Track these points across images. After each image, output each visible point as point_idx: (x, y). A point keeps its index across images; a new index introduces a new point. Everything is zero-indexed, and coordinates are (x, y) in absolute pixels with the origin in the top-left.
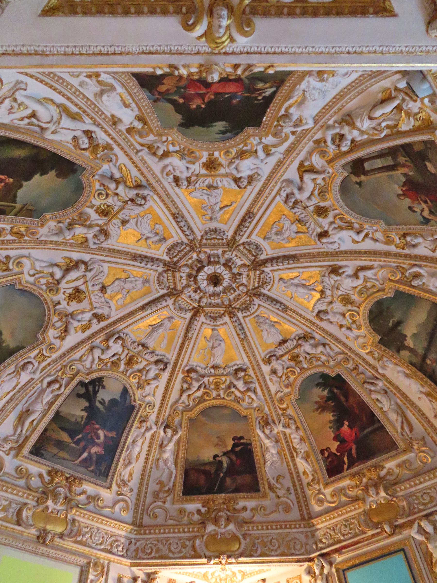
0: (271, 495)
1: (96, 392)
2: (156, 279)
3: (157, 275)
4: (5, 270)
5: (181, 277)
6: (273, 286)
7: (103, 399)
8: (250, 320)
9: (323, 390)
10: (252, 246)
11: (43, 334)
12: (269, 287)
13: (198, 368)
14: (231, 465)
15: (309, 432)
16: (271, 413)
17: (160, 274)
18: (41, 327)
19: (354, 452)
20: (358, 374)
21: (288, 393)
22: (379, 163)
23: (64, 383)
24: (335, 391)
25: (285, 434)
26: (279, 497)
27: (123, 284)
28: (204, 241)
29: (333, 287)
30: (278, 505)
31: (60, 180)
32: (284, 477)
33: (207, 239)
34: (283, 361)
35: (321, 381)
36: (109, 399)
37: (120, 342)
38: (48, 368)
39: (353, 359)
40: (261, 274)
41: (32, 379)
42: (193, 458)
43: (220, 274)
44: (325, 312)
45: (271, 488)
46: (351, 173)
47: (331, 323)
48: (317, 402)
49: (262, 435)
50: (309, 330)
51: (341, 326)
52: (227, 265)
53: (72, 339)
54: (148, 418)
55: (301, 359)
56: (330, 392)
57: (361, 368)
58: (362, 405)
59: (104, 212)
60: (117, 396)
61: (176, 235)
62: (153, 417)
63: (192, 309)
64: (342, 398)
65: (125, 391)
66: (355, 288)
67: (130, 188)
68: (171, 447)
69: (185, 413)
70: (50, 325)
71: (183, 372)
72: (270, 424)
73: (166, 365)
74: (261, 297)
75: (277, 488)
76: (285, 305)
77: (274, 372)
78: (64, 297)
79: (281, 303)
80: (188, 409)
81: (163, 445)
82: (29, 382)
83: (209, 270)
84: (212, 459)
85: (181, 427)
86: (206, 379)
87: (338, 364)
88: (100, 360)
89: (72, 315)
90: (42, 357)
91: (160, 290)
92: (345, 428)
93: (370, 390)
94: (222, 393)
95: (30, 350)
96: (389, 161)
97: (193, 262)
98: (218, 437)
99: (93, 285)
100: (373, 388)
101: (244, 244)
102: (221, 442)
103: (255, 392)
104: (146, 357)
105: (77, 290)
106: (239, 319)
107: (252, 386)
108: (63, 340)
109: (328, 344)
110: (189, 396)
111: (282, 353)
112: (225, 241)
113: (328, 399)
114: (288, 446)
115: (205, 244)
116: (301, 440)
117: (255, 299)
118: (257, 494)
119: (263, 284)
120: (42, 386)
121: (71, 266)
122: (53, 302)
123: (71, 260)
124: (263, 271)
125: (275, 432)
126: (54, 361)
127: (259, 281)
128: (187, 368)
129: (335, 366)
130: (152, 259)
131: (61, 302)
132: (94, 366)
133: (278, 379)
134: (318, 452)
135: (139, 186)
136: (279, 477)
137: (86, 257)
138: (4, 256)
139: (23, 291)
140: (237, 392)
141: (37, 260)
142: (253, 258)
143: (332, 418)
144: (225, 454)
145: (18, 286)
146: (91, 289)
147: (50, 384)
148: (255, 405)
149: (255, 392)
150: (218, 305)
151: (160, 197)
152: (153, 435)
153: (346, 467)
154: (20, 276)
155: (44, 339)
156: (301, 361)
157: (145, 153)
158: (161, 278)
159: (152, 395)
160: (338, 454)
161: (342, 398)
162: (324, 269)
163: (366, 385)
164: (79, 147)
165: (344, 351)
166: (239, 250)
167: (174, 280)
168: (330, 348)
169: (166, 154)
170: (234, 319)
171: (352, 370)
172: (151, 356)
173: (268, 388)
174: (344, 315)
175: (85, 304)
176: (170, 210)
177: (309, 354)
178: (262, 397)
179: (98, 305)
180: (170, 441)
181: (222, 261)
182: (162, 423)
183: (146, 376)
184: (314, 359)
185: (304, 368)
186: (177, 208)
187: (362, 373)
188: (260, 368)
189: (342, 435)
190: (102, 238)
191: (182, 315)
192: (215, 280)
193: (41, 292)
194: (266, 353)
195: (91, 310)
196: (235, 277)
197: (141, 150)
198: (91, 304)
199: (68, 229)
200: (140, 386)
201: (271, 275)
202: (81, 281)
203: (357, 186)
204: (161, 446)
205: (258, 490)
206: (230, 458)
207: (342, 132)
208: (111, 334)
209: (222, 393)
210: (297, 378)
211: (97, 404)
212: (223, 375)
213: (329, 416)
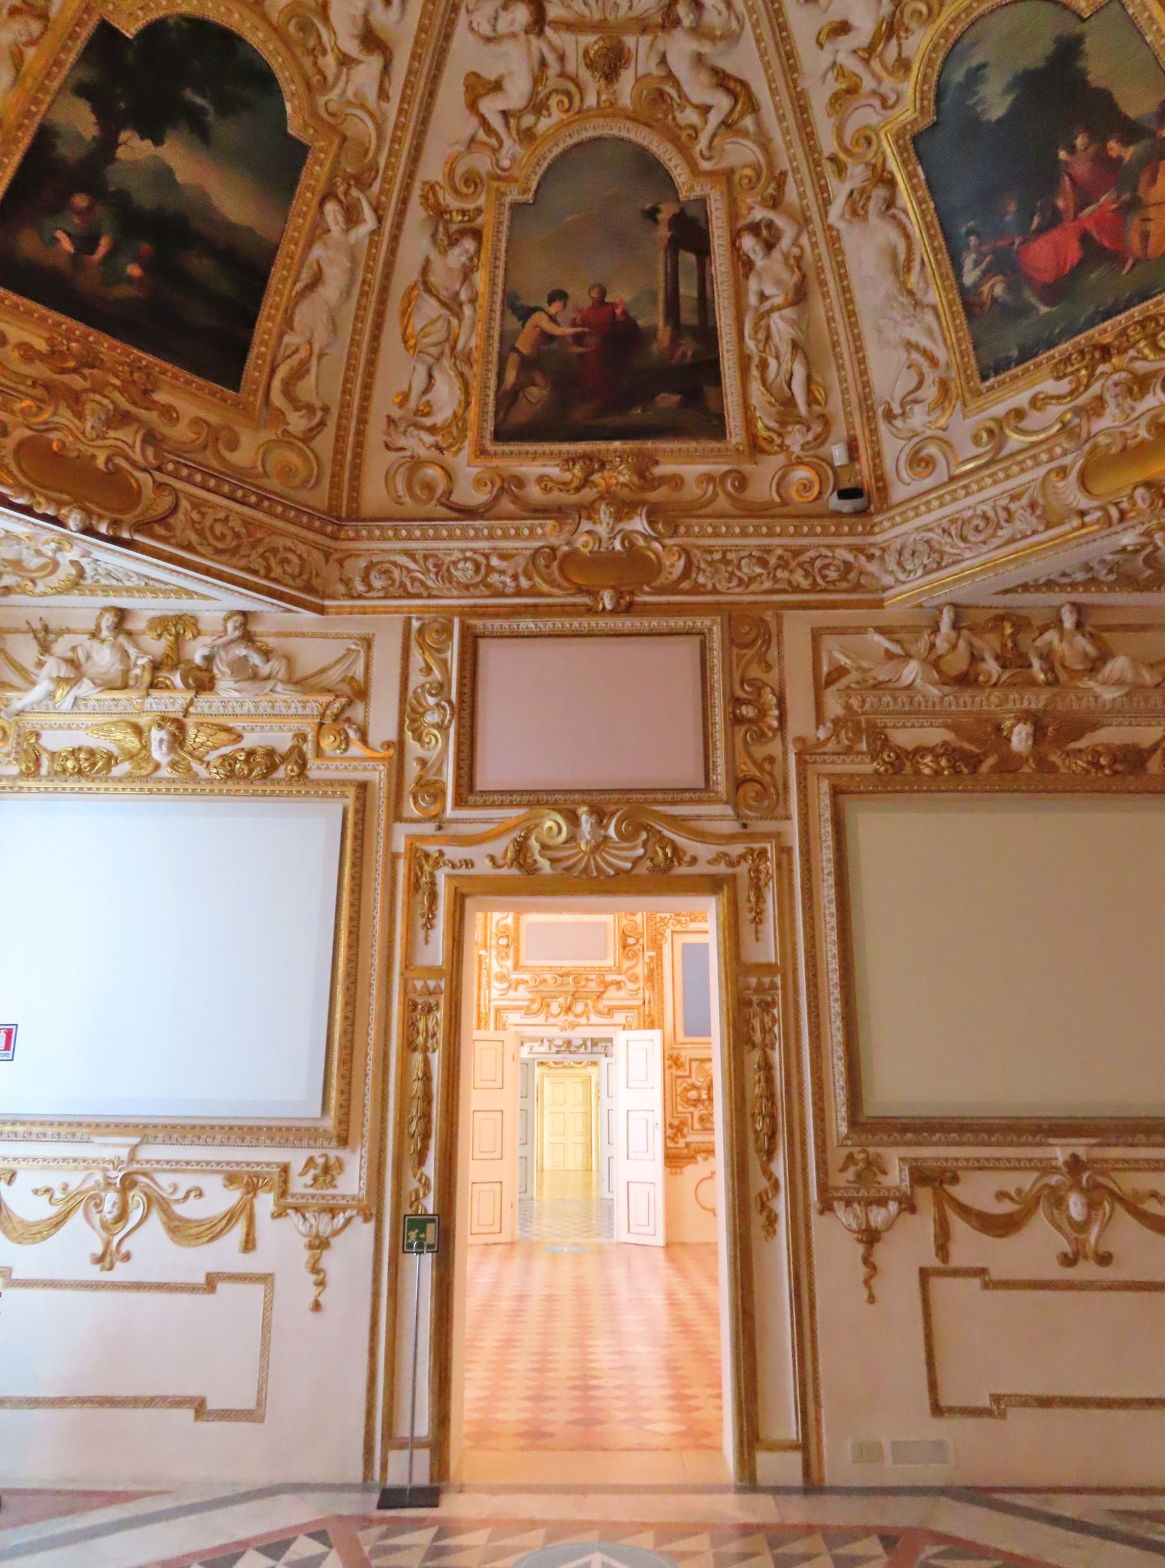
22: (688, 290)
46: (682, 211)
96: (688, 317)
203: (648, 206)
207: (776, 254)
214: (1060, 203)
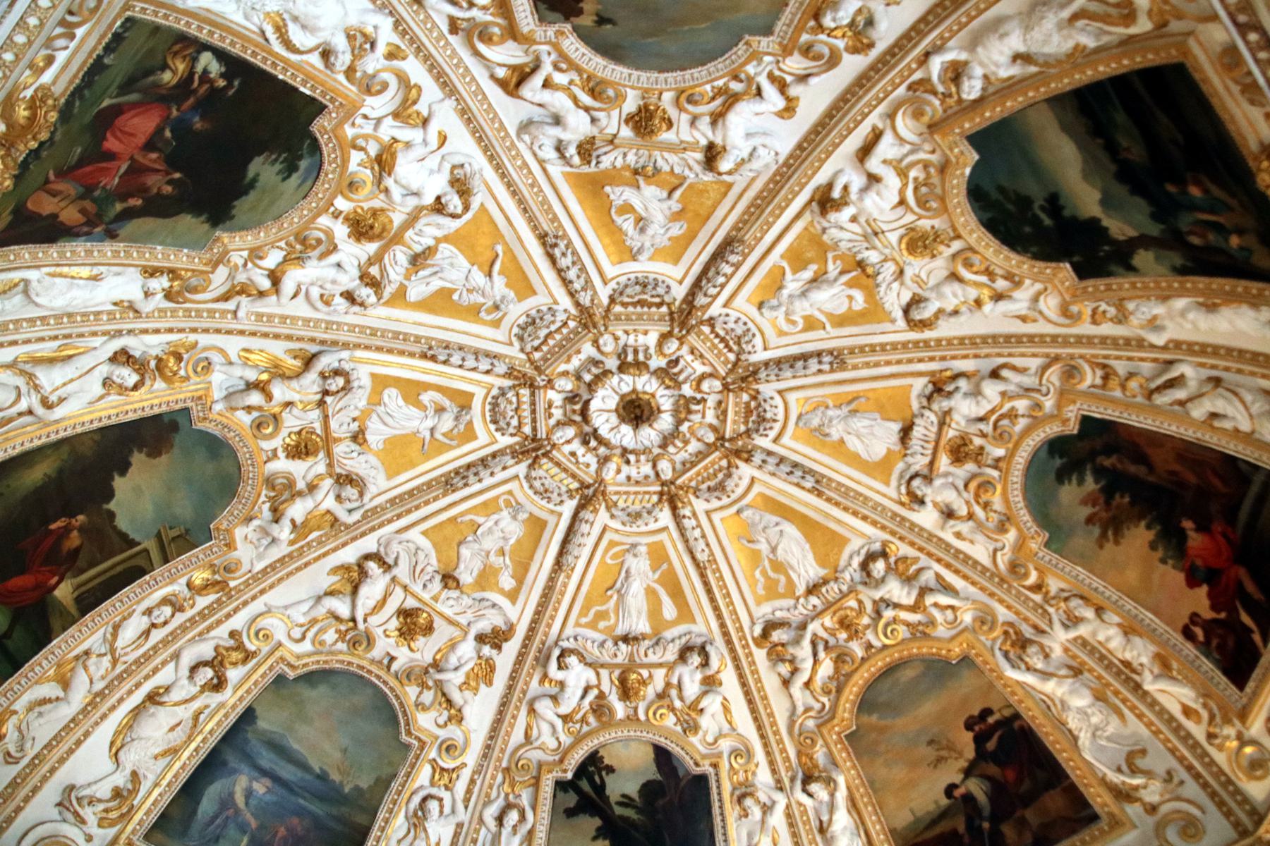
0: (1133, 810)
1: (600, 789)
2: (530, 492)
3: (526, 485)
4: (245, 660)
5: (573, 454)
6: (762, 334)
7: (624, 796)
8: (795, 437)
9: (1081, 482)
10: (629, 291)
11: (409, 733)
12: (758, 341)
13: (779, 614)
14: (997, 790)
15: (1129, 605)
16: (1017, 613)
17: (527, 477)
18: (397, 723)
19: (1250, 587)
20: (1123, 387)
21: (1017, 541)
23: (525, 801)
24: (1107, 462)
25: (1084, 643)
26: (1152, 809)
27: (476, 546)
28: (537, 355)
29: (865, 236)
30: (1160, 828)
31: (164, 458)
32: (1143, 752)
33: (537, 349)
34: (946, 475)
35: (1058, 462)
36: (637, 787)
37: (572, 660)
38: (476, 790)
39: (1081, 357)
40: (713, 327)
41: (460, 826)
42: (903, 819)
43: (634, 391)
44: (916, 301)
45: (1124, 795)
47: (956, 312)
48: (1090, 520)
49: (1029, 679)
50: (934, 366)
51: (978, 303)
52: (630, 363)
53: (480, 709)
54: (753, 785)
55: (978, 441)
56: (1099, 473)
57: (1121, 367)
58: (1191, 454)
59: (300, 450)
60: (652, 773)
61: (479, 385)
62: (763, 777)
63: (660, 501)
64: (1133, 469)
65: (662, 756)
66: (902, 202)
67: (298, 376)
68: (842, 820)
69: (825, 731)
70: (411, 709)
71: (758, 645)
72: (1031, 642)
73: (703, 651)
74: (762, 375)
75: (1136, 788)
76: (831, 352)
77: (949, 514)
78: (392, 641)
79: (819, 354)
80: (826, 718)
81: (825, 825)
82: (456, 835)
83: (604, 402)
84: (945, 802)
85: (835, 764)
86: (814, 627)
87: (1064, 395)
88: (565, 718)
89: (436, 665)
90: (445, 775)
91: (558, 509)
92: (1195, 540)
93: (1182, 403)
94: (870, 636)
95: (408, 775)
97: (563, 407)
98: (931, 742)
99: (425, 586)
100: (1180, 394)
101: (612, 300)
102: (941, 748)
103: (948, 589)
104: (653, 658)
105: (406, 614)
106: (770, 453)
107: (927, 578)
108: (462, 719)
109: (1004, 366)
110: (807, 685)
111: (927, 460)
112: (572, 324)
113: (1108, 493)
114: (1109, 666)
115: (545, 359)
116: (1126, 634)
117: (761, 387)
118: (1094, 830)
119: (739, 344)
120: (489, 830)
121: (354, 577)
122: (380, 662)
123: (345, 568)
124: (711, 319)
125: (1057, 652)
126: (478, 770)
127: (727, 346)
128: (758, 630)
129: (1059, 406)
130: (483, 462)
131: (393, 653)
132: (563, 738)
133: (971, 523)
134: (1178, 638)
135: (309, 361)
136: (1130, 758)
137: (369, 544)
138: (226, 636)
139: (311, 678)
140: (904, 615)
141: (286, 607)
142: (664, 309)
143: (1150, 535)
144: (968, 773)
145: (291, 674)
146: (426, 596)
147: (500, 820)
148: (967, 618)
149: (948, 589)
150: (701, 456)
151: (367, 348)
152: (789, 815)
153: (1257, 638)
154: (278, 654)
155: (419, 740)
156: (982, 448)
157: (245, 305)
158: (537, 484)
159: (721, 728)
160: (1223, 615)
161: (1133, 469)
162: (807, 216)
163: (1160, 400)
164: (126, 389)
165: (1047, 356)
166: (618, 318)
167: (565, 470)
168: (1014, 368)
169: (275, 278)
170: (757, 458)
171: (1104, 386)
172: (659, 650)
173: (967, 559)
174: (954, 277)
175: (443, 632)
176: (412, 355)
177: (981, 419)
178: (972, 589)
179: (470, 616)
180: (832, 807)
181: (612, 363)
182: (792, 780)
183: (681, 699)
184: (1005, 422)
185: (998, 460)
186: (418, 339)
187: (1131, 375)
188: (913, 525)
189: (1199, 562)
190: (350, 492)
191: (653, 526)
192: (636, 411)
193: (341, 657)
194: (894, 483)
195: (466, 633)
196: (668, 375)
197: (238, 306)
198: (451, 622)
199: (277, 522)
200: (691, 727)
201: (734, 315)
202: (399, 593)
204: (822, 830)
205: (1095, 818)
206: (984, 776)
208: (542, 654)
209: (870, 636)
210: (1010, 493)
211: (619, 811)
212: (844, 596)
213: (1140, 536)
214: (154, 156)
